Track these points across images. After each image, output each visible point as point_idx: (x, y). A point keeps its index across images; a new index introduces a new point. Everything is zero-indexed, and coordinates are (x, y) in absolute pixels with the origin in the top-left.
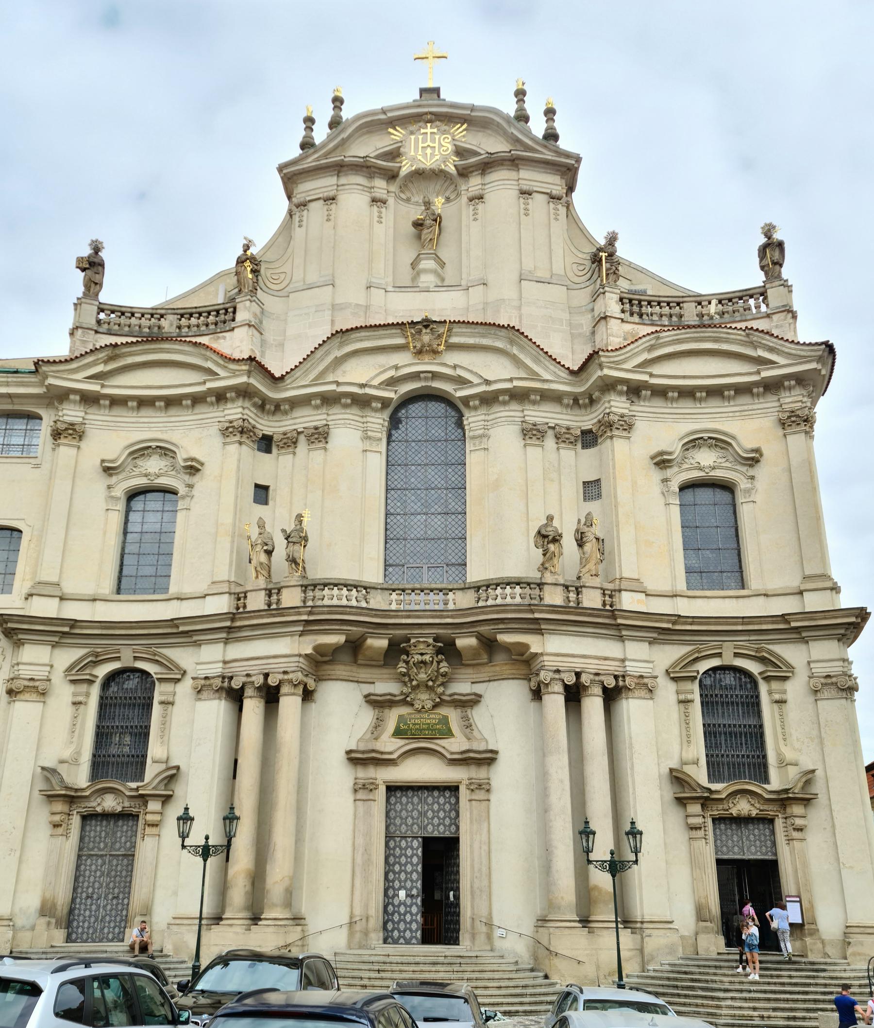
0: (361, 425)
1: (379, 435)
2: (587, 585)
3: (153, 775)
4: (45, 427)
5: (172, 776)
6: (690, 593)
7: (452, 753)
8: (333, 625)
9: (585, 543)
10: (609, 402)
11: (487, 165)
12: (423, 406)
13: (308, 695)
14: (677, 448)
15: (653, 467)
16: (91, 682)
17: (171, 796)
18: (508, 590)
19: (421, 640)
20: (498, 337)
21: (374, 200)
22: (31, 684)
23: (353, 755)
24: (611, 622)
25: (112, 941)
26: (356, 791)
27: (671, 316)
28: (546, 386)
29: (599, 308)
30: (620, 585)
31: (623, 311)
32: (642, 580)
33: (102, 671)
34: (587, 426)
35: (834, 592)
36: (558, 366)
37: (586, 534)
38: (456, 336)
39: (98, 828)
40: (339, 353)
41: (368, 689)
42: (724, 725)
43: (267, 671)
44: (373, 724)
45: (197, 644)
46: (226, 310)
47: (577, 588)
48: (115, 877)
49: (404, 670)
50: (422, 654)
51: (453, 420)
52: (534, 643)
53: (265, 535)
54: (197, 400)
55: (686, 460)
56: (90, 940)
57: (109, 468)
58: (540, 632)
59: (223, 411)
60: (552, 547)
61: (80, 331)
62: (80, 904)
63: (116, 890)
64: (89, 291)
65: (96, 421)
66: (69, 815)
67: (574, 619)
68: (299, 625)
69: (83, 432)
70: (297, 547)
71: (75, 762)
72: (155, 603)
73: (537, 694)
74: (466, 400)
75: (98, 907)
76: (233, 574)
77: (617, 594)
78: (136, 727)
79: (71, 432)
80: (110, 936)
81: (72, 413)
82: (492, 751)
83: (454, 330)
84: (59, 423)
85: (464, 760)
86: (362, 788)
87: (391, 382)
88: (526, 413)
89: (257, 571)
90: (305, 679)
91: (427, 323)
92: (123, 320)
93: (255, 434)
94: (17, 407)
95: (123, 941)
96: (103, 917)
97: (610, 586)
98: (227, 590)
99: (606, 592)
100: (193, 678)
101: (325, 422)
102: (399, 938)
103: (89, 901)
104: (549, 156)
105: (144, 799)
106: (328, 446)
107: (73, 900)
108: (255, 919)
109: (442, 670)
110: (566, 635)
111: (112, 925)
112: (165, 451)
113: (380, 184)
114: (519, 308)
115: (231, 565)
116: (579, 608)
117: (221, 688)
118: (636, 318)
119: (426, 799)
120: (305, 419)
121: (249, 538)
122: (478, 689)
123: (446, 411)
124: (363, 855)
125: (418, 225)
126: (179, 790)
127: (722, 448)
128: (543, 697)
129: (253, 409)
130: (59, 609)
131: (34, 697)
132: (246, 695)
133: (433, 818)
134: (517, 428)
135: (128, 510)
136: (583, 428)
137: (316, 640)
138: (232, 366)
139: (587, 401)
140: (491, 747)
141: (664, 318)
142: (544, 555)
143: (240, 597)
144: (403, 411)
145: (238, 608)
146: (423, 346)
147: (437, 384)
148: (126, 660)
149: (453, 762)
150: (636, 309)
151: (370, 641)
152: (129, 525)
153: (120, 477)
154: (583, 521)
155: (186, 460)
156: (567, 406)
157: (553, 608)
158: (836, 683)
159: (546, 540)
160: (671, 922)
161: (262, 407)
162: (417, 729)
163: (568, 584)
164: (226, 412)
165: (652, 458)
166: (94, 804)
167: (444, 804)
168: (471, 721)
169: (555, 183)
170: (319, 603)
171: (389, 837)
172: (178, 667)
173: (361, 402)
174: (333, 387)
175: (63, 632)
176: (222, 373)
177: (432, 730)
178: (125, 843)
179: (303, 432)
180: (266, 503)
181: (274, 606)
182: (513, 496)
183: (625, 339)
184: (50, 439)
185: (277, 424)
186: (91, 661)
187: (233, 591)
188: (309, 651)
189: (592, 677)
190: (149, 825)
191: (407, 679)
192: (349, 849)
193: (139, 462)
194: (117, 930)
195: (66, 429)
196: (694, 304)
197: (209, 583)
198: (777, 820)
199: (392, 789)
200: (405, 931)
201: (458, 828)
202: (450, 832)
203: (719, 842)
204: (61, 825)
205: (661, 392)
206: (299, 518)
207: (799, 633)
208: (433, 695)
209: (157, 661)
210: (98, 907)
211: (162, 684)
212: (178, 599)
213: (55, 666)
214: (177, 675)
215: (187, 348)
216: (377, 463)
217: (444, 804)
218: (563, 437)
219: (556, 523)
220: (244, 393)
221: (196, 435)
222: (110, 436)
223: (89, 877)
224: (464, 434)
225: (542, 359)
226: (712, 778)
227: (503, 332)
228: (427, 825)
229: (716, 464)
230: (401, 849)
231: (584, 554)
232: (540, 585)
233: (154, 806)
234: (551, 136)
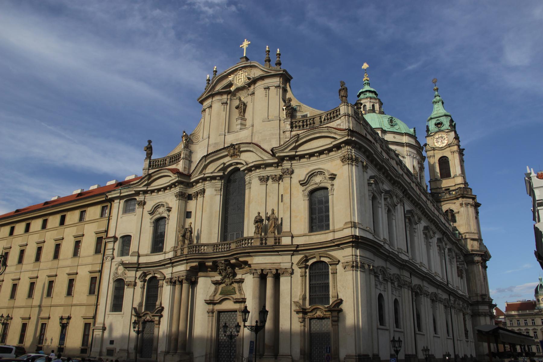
11: (254, 81)
13: (193, 284)
20: (250, 147)
21: (222, 104)
24: (276, 249)
33: (148, 278)
45: (167, 268)
52: (249, 260)
54: (170, 187)
67: (264, 249)
71: (140, 305)
82: (242, 299)
87: (224, 169)
91: (232, 146)
104: (273, 73)
113: (225, 97)
120: (200, 186)
122: (244, 276)
125: (237, 108)
143: (176, 252)
149: (235, 302)
156: (275, 167)
157: (256, 247)
169: (276, 81)
173: (213, 178)
174: (202, 176)
175: (137, 266)
188: (188, 269)
199: (220, 312)
205: (302, 157)
227: (251, 145)
234: (279, 64)
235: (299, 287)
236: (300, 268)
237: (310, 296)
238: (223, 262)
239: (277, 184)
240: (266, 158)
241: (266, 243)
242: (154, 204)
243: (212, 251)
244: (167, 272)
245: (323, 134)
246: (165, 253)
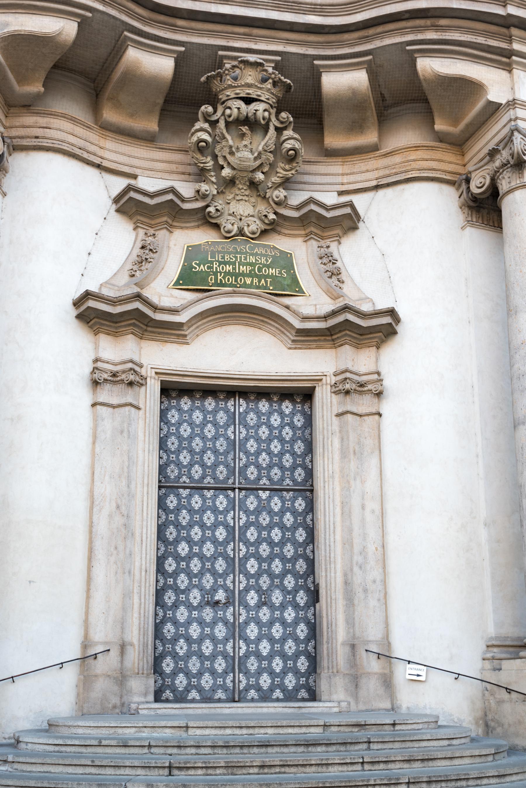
7: (306, 318)
102: (187, 690)
109: (288, 145)
124: (110, 516)
162: (227, 273)
171: (166, 486)
177: (260, 278)
200: (200, 674)
208: (262, 207)
228: (246, 466)
230: (191, 511)
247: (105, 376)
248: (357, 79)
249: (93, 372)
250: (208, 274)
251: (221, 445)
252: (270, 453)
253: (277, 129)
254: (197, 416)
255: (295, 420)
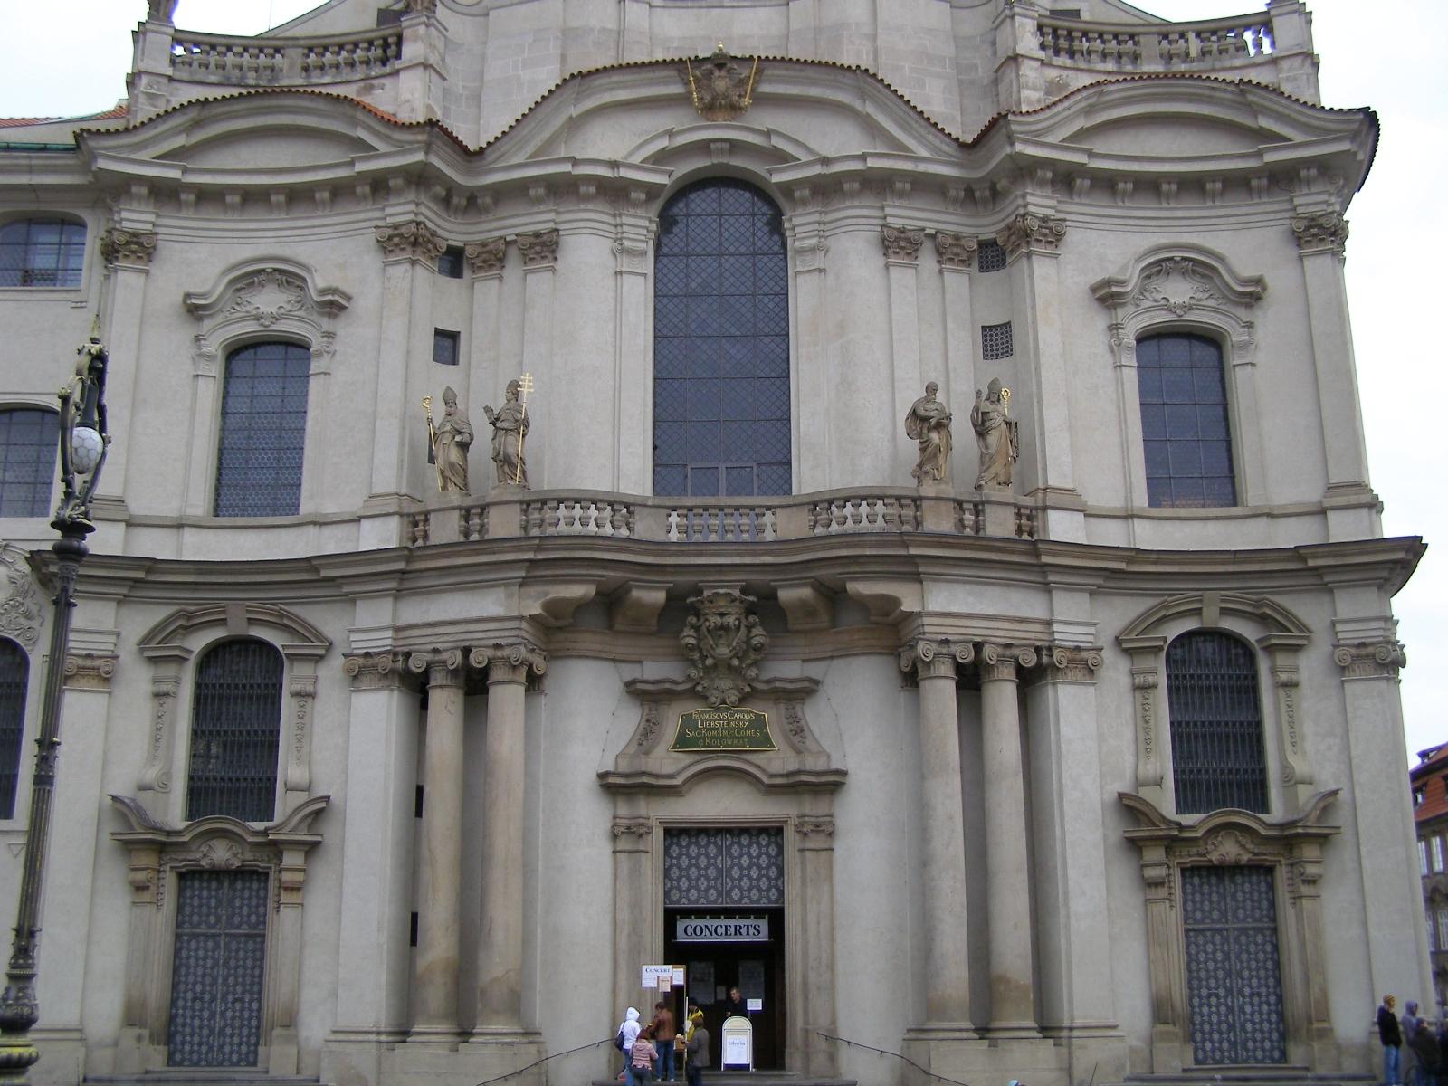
0: (613, 229)
1: (642, 246)
2: (993, 499)
3: (289, 811)
4: (92, 242)
5: (319, 812)
6: (1155, 512)
7: (772, 776)
8: (574, 567)
9: (989, 429)
10: (1024, 196)
12: (714, 195)
13: (534, 682)
14: (1133, 276)
15: (1095, 305)
16: (181, 660)
17: (319, 843)
18: (864, 508)
19: (722, 591)
22: (89, 663)
23: (611, 780)
24: (1031, 560)
25: (238, 1064)
26: (615, 837)
27: (1120, 56)
28: (922, 167)
29: (1004, 35)
30: (1044, 500)
31: (1043, 47)
32: (1078, 491)
33: (199, 642)
34: (988, 234)
35: (1374, 511)
36: (940, 135)
37: (991, 415)
38: (770, 82)
39: (205, 893)
40: (575, 111)
41: (631, 672)
42: (1203, 724)
43: (467, 644)
44: (641, 729)
45: (351, 600)
46: (385, 40)
47: (976, 505)
48: (237, 967)
49: (692, 641)
50: (722, 615)
51: (765, 219)
53: (456, 418)
54: (340, 192)
55: (1147, 294)
56: (203, 1063)
57: (198, 307)
58: (917, 578)
59: (383, 209)
60: (935, 436)
61: (145, 79)
62: (185, 1008)
63: (239, 989)
64: (158, 11)
65: (172, 227)
66: (159, 871)
67: (973, 555)
68: (520, 569)
69: (154, 248)
70: (511, 438)
72: (277, 531)
73: (911, 679)
74: (788, 189)
75: (212, 1016)
76: (404, 484)
77: (1040, 514)
78: (256, 732)
79: (134, 247)
80: (235, 1057)
81: (135, 217)
83: (766, 72)
84: (116, 234)
85: (793, 786)
86: (626, 834)
87: (662, 158)
88: (888, 211)
89: (445, 478)
90: (530, 657)
91: (720, 62)
92: (213, 58)
93: (435, 247)
94: (44, 207)
95: (255, 1064)
96: (222, 1030)
97: (1029, 501)
98: (396, 510)
99: (1022, 511)
100: (345, 655)
101: (552, 225)
103: (198, 1005)
105: (276, 848)
106: (559, 266)
107: (173, 1002)
108: (465, 1034)
109: (755, 641)
110: (958, 582)
111: (236, 1040)
112: (288, 277)
114: (874, 37)
115: (401, 467)
116: (980, 540)
117: (393, 671)
118: (1064, 60)
119: (729, 848)
121: (430, 421)
122: (814, 670)
123: (753, 205)
126: (329, 833)
127: (1203, 276)
128: (922, 684)
129: (431, 205)
130: (127, 542)
131: (93, 684)
132: (432, 683)
133: (740, 879)
134: (873, 235)
135: (228, 375)
136: (981, 237)
137: (547, 594)
138: (398, 135)
139: (987, 193)
140: (835, 765)
141: (1124, 59)
142: (923, 450)
143: (417, 521)
144: (681, 205)
145: (415, 540)
146: (714, 99)
147: (737, 162)
148: (237, 626)
150: (1063, 43)
151: (635, 593)
152: (230, 401)
153: (219, 319)
154: (984, 395)
155: (323, 292)
156: (955, 201)
157: (940, 540)
158: (1374, 656)
159: (926, 425)
160: (1114, 1027)
161: (446, 202)
162: (713, 737)
163: (959, 497)
164: (389, 211)
165: (1094, 289)
166: (199, 856)
167: (759, 857)
168: (802, 722)
170: (551, 531)
172: (319, 636)
173: (614, 192)
174: (567, 168)
175: (137, 579)
176: (382, 147)
178: (249, 915)
179: (514, 242)
180: (454, 361)
181: (475, 537)
182: (869, 355)
183: (1048, 93)
184: (98, 260)
185: (474, 229)
186: (181, 627)
187: (406, 511)
188: (536, 610)
189: (1000, 650)
190: (286, 889)
191: (696, 656)
192: (607, 929)
193: (245, 296)
194: (244, 1048)
195: (127, 243)
196: (1156, 39)
197: (366, 498)
198: (1278, 867)
199: (674, 833)
201: (781, 893)
202: (770, 901)
203: (1190, 904)
204: (148, 887)
205: (1107, 184)
206: (514, 390)
207: (1320, 576)
208: (740, 683)
209: (286, 626)
210: (212, 1016)
211: (296, 664)
212: (315, 523)
213: (124, 634)
214: (317, 649)
215: (321, 105)
216: (639, 294)
217: (759, 857)
218: (948, 251)
219: (940, 397)
220: (419, 178)
221: (336, 251)
222: (199, 256)
223: (196, 967)
224: (784, 245)
225: (915, 125)
226: (1182, 806)
227: (848, 79)
229: (1193, 302)
231: (987, 448)
232: (917, 501)
233: (292, 859)
235: (1128, 734)
236: (1130, 653)
237: (1175, 771)
238: (736, 593)
239: (967, 277)
240: (924, 153)
241: (978, 527)
242: (233, 260)
243: (660, 536)
244: (369, 624)
245: (1205, 110)
246: (320, 523)
247: (622, 829)
248: (806, 593)
249: (613, 827)
250: (698, 739)
251: (712, 872)
252: (750, 878)
253: (746, 627)
254: (693, 850)
255: (770, 850)
